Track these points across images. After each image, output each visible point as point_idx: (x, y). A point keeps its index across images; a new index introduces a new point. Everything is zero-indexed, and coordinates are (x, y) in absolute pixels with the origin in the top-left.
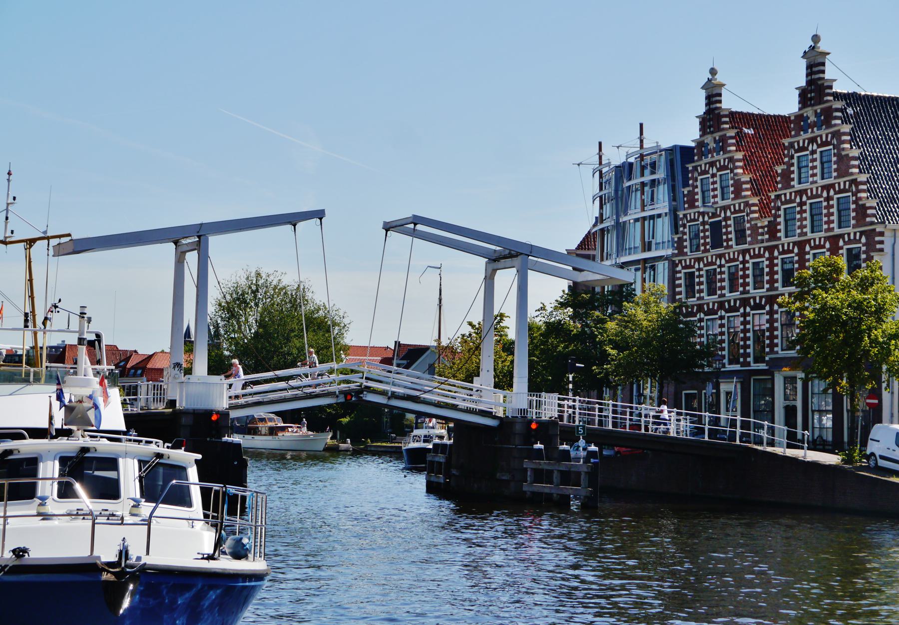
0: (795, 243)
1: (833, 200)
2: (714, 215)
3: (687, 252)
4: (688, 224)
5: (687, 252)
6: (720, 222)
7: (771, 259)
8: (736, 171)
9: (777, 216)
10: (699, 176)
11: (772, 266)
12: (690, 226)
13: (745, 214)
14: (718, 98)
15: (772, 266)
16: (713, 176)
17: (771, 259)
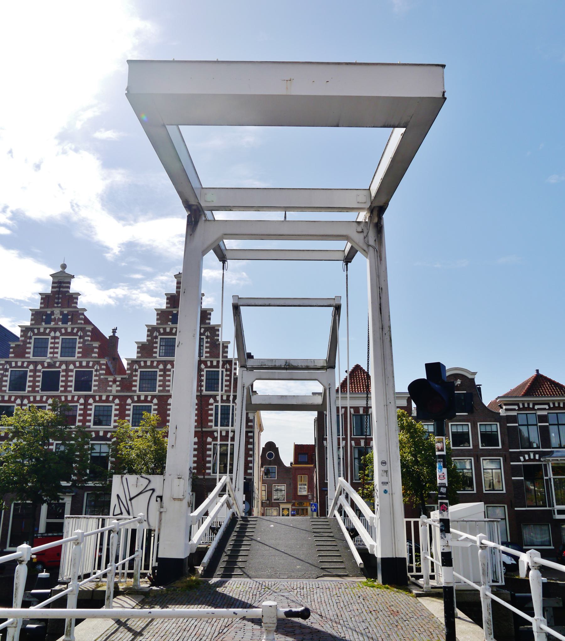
0: (153, 397)
1: (203, 371)
2: (50, 365)
3: (6, 390)
4: (10, 369)
5: (6, 390)
6: (59, 372)
7: (86, 404)
8: (86, 338)
9: (131, 375)
10: (33, 335)
11: (85, 409)
12: (11, 371)
13: (94, 370)
14: (67, 285)
15: (85, 409)
16: (55, 338)
17: (86, 404)
